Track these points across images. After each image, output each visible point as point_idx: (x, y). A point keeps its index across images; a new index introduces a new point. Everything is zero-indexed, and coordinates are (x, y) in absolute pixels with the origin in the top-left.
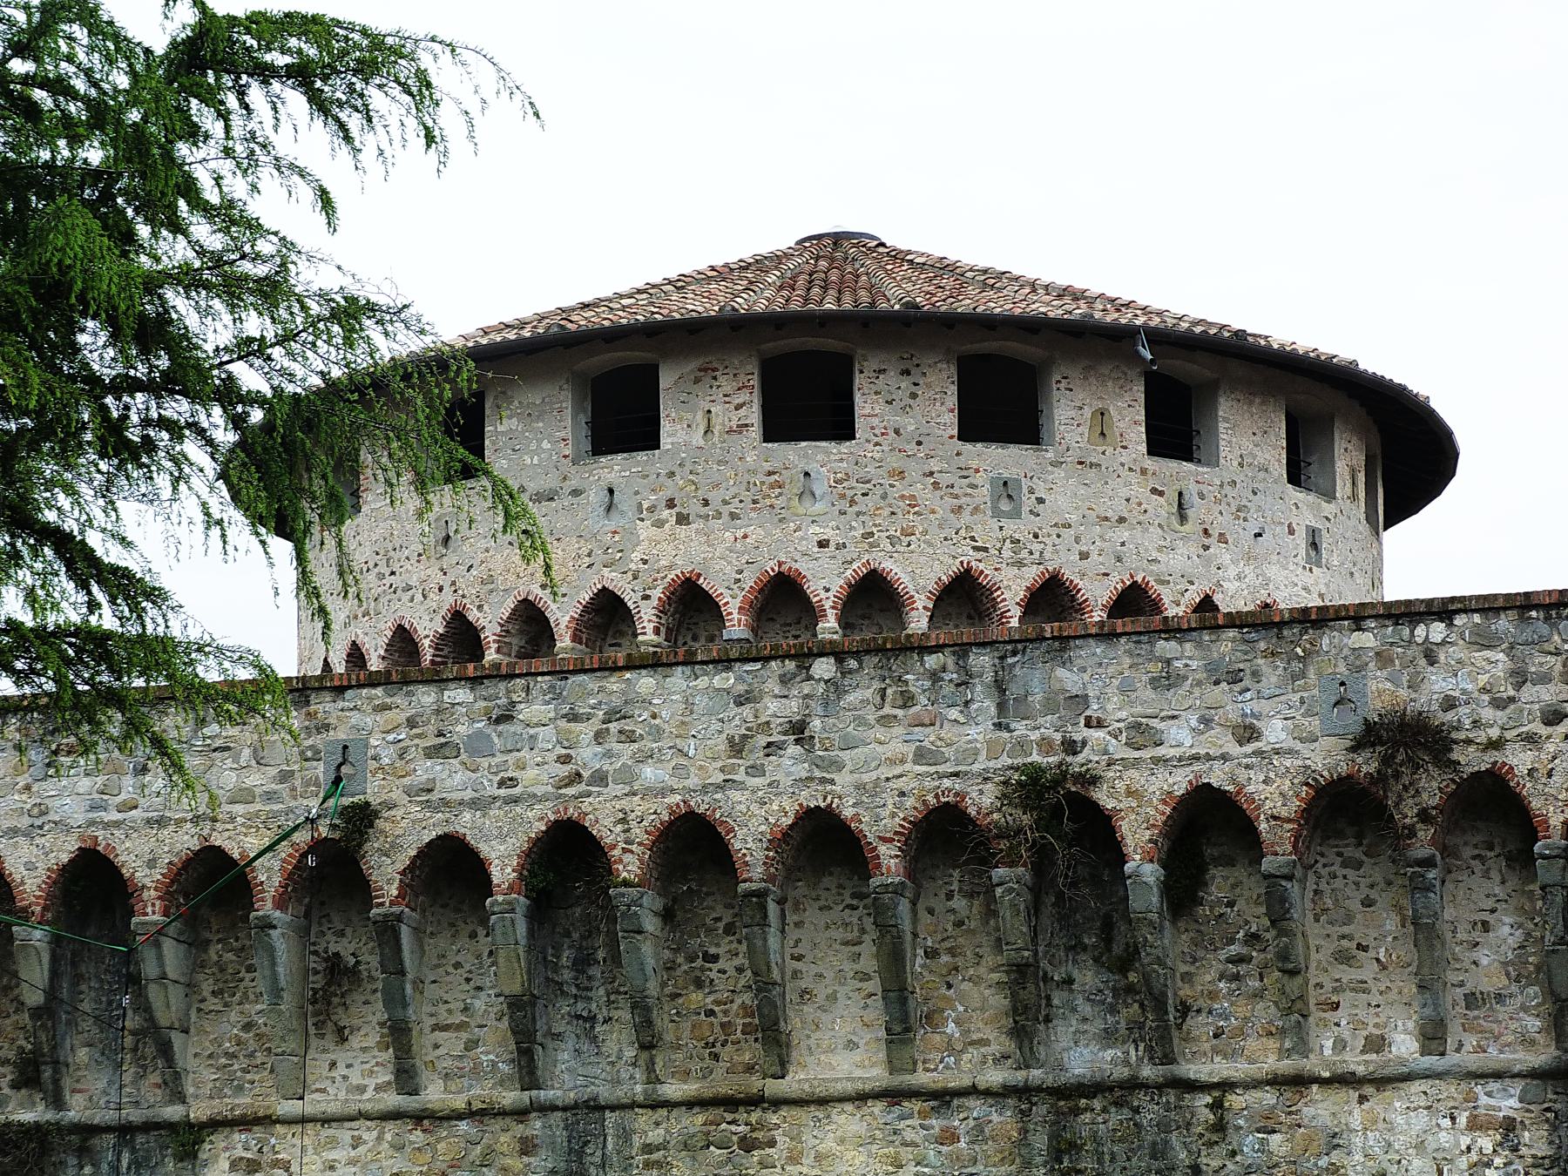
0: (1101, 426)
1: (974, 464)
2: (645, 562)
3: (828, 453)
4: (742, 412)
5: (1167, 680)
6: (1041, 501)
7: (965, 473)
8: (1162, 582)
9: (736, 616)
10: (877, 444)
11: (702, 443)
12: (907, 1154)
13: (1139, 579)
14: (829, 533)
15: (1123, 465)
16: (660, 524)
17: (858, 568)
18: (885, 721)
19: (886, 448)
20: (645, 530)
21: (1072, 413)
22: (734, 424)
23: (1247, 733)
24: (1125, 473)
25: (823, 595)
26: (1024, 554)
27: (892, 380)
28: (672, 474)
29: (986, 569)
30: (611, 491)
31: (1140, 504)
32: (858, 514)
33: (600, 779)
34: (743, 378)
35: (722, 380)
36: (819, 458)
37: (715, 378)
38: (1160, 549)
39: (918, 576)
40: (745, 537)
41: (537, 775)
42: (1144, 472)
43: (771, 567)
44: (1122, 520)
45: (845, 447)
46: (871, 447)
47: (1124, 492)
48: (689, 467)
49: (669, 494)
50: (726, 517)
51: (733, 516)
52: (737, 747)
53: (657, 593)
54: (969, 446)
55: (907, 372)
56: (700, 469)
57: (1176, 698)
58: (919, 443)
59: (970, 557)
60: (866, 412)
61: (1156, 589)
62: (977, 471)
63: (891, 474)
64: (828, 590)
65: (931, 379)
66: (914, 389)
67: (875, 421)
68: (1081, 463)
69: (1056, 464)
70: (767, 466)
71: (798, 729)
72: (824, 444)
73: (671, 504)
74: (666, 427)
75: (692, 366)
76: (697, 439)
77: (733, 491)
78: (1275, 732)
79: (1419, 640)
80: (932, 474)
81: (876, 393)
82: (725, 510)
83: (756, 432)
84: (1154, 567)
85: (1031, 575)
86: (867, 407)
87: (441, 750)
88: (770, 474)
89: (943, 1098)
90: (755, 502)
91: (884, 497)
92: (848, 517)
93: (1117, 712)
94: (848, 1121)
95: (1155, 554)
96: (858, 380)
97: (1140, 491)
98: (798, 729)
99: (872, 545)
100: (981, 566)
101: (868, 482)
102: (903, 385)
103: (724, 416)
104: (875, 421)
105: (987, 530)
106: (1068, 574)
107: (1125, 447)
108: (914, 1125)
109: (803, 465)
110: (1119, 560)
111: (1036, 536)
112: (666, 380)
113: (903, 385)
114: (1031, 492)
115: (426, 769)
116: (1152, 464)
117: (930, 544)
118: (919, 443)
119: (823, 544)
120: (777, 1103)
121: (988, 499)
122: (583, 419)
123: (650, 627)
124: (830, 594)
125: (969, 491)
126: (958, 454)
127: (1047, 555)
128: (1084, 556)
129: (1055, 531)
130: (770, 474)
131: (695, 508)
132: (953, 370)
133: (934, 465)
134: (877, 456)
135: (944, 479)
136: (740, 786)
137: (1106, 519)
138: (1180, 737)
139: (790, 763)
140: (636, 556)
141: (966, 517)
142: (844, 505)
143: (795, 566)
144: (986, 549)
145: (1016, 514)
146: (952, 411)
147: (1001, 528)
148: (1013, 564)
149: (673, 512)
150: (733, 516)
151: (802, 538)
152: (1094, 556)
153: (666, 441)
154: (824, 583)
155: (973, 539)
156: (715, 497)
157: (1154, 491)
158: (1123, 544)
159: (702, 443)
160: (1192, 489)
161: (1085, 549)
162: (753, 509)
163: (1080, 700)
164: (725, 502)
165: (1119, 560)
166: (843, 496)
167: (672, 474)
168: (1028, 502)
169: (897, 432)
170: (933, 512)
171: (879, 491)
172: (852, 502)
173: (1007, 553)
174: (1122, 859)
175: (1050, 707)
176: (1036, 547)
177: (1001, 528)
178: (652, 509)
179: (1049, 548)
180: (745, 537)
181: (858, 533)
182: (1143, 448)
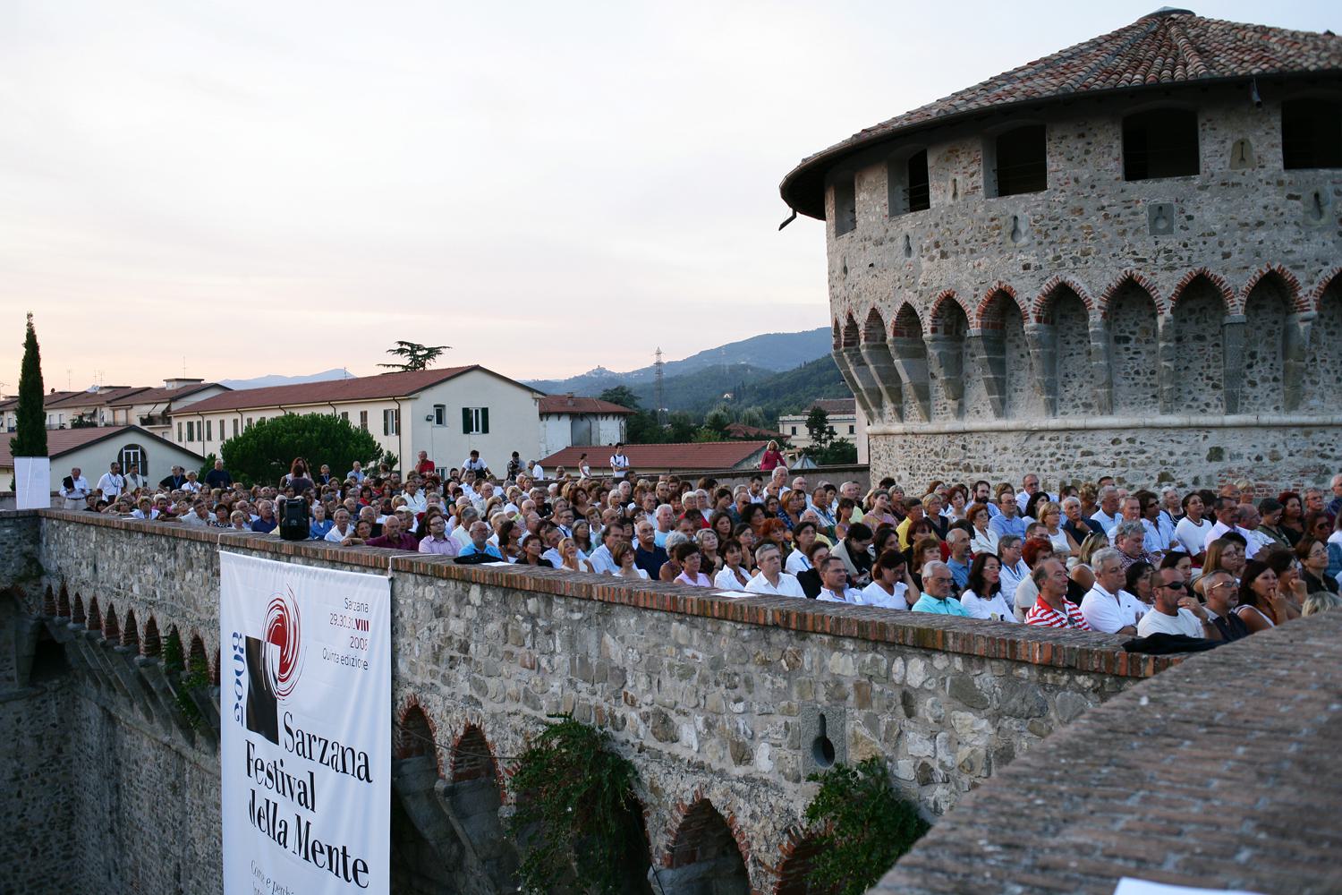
0: (1242, 153)
1: (1135, 197)
2: (925, 284)
3: (1028, 201)
4: (975, 178)
6: (1190, 218)
7: (1129, 204)
8: (1296, 267)
9: (975, 320)
10: (1062, 191)
11: (952, 202)
13: (1275, 267)
14: (1032, 260)
15: (1260, 181)
16: (932, 259)
17: (1051, 282)
19: (1068, 193)
20: (925, 264)
21: (1216, 147)
22: (969, 187)
24: (1262, 187)
25: (1027, 303)
26: (1175, 260)
27: (1075, 145)
28: (937, 225)
29: (1145, 276)
30: (908, 237)
31: (1276, 209)
32: (1052, 243)
34: (973, 154)
35: (962, 158)
36: (1023, 205)
37: (957, 156)
38: (1296, 242)
39: (1093, 285)
40: (979, 265)
42: (1280, 183)
43: (994, 285)
44: (1260, 224)
45: (1041, 196)
46: (1058, 194)
47: (1263, 201)
48: (945, 220)
49: (936, 237)
50: (968, 252)
51: (972, 251)
53: (931, 306)
54: (1131, 184)
55: (1082, 136)
56: (952, 220)
58: (1093, 187)
59: (1132, 267)
60: (1054, 168)
61: (1290, 274)
62: (1138, 202)
63: (1074, 212)
64: (1029, 300)
65: (1100, 137)
66: (1087, 147)
67: (1060, 175)
68: (1223, 184)
69: (1203, 188)
70: (991, 215)
72: (1025, 195)
73: (937, 245)
74: (933, 193)
75: (945, 149)
76: (949, 199)
77: (971, 233)
79: (897, 678)
80: (1103, 208)
81: (1061, 154)
82: (968, 247)
83: (981, 192)
84: (1290, 257)
85: (1182, 275)
86: (1055, 165)
88: (992, 220)
90: (984, 240)
91: (1069, 228)
92: (1043, 246)
95: (1289, 247)
96: (1050, 146)
97: (1275, 197)
99: (1059, 265)
100: (1141, 273)
101: (1057, 219)
102: (1079, 146)
103: (964, 183)
104: (1060, 175)
105: (1145, 246)
106: (1212, 271)
107: (1263, 167)
109: (1012, 212)
110: (1258, 254)
111: (1185, 245)
112: (931, 162)
113: (1079, 146)
114: (1182, 211)
116: (1286, 176)
117: (1104, 261)
118: (1093, 187)
119: (1026, 267)
121: (1146, 222)
122: (900, 189)
123: (929, 328)
124: (1032, 303)
125: (1131, 217)
126: (1122, 191)
127: (1194, 259)
128: (1226, 256)
129: (1202, 239)
130: (992, 220)
131: (950, 247)
132: (1118, 130)
133: (1105, 202)
134: (1062, 200)
135: (1115, 210)
137: (1247, 224)
140: (921, 281)
141: (1129, 238)
142: (1038, 238)
143: (1008, 284)
144: (1144, 260)
145: (1169, 230)
146: (1117, 159)
147: (1157, 243)
148: (1166, 269)
149: (939, 250)
150: (972, 251)
151: (1012, 265)
152: (1235, 256)
153: (933, 202)
154: (1027, 295)
155: (1134, 253)
156: (962, 238)
157: (1291, 197)
158: (1261, 242)
159: (952, 202)
160: (1328, 189)
161: (1227, 250)
162: (984, 246)
164: (967, 242)
165: (1258, 254)
166: (1040, 232)
167: (937, 225)
168: (1179, 220)
169: (1076, 180)
170: (1104, 236)
171: (1065, 225)
172: (1047, 235)
173: (1161, 261)
174: (649, 863)
176: (1185, 254)
177: (1157, 243)
178: (928, 249)
179: (1196, 254)
180: (979, 265)
181: (1050, 257)
182: (1280, 165)
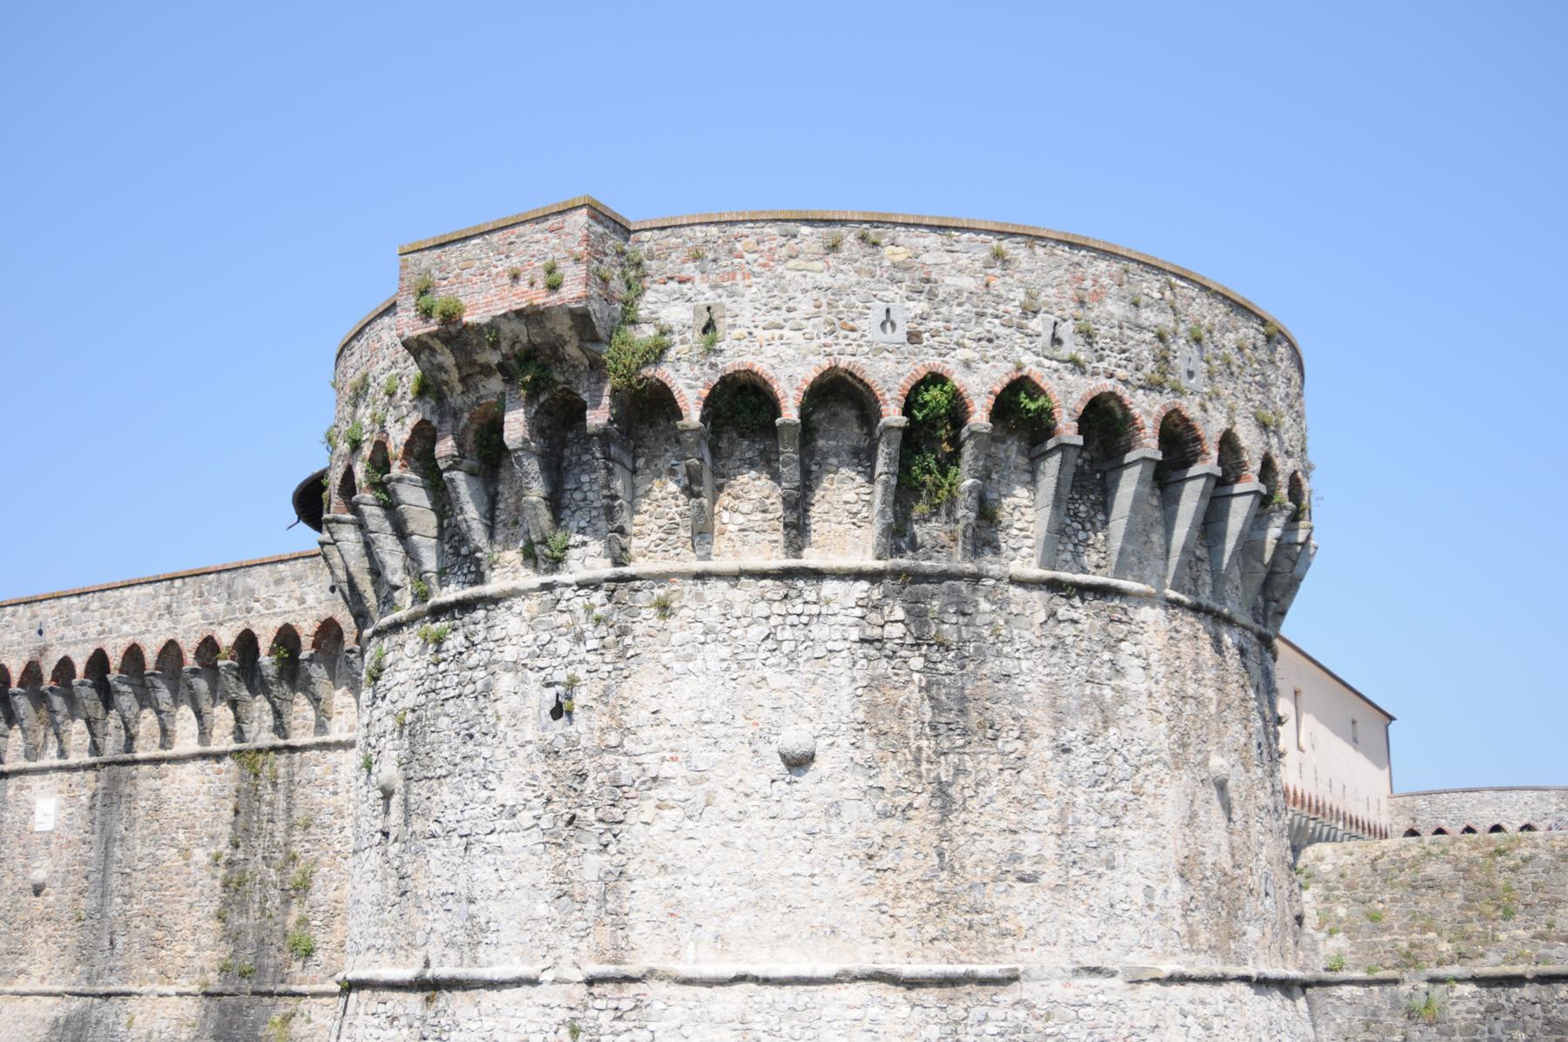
5: (279, 582)
12: (206, 779)
18: (194, 603)
23: (302, 601)
33: (110, 631)
41: (93, 631)
52: (151, 616)
57: (283, 588)
71: (169, 607)
78: (310, 600)
87: (68, 623)
89: (218, 757)
93: (263, 593)
94: (191, 767)
98: (169, 607)
108: (210, 766)
115: (62, 630)
120: (170, 760)
136: (148, 631)
138: (281, 603)
139: (165, 623)
163: (252, 591)
175: (243, 595)
